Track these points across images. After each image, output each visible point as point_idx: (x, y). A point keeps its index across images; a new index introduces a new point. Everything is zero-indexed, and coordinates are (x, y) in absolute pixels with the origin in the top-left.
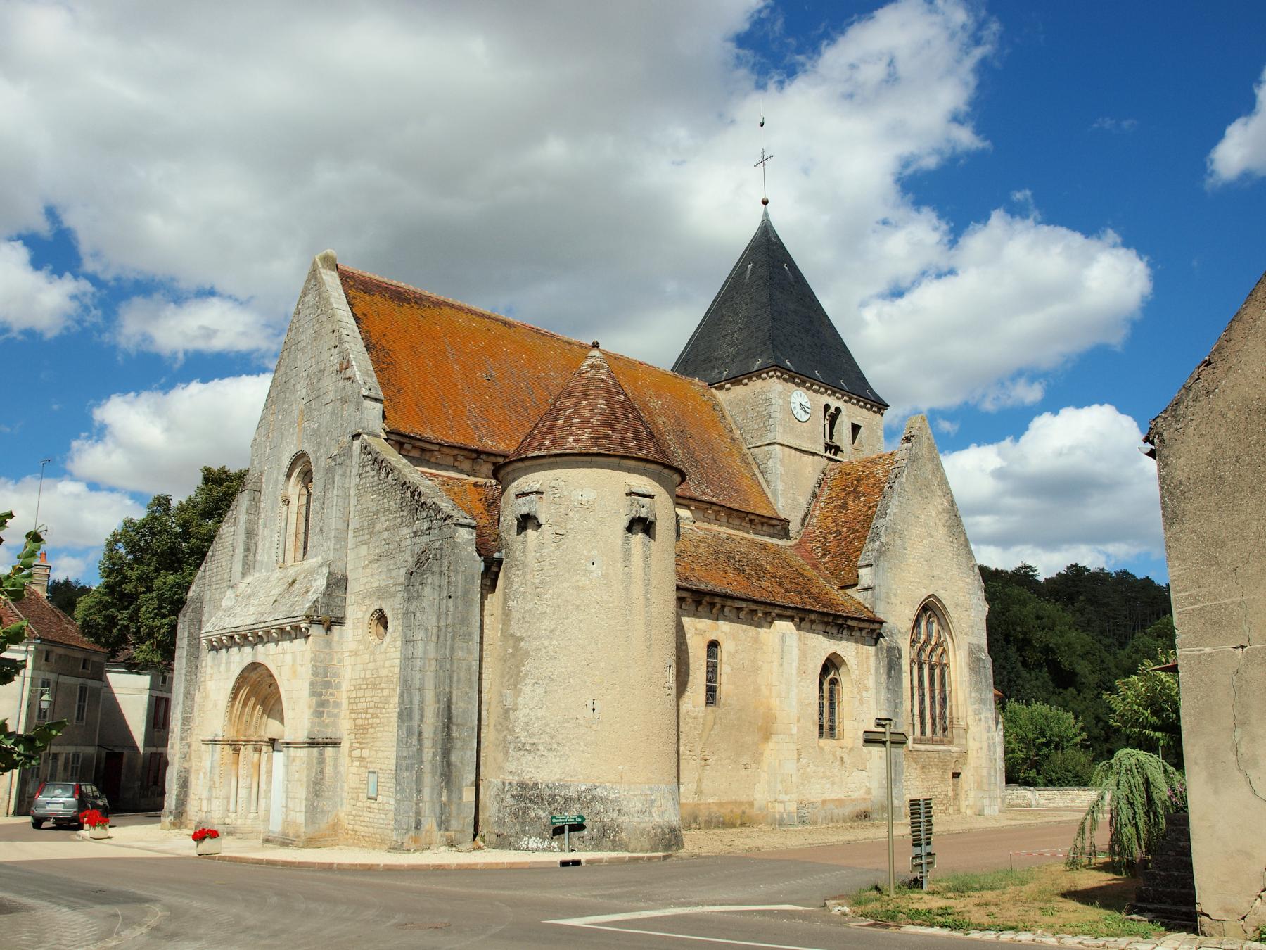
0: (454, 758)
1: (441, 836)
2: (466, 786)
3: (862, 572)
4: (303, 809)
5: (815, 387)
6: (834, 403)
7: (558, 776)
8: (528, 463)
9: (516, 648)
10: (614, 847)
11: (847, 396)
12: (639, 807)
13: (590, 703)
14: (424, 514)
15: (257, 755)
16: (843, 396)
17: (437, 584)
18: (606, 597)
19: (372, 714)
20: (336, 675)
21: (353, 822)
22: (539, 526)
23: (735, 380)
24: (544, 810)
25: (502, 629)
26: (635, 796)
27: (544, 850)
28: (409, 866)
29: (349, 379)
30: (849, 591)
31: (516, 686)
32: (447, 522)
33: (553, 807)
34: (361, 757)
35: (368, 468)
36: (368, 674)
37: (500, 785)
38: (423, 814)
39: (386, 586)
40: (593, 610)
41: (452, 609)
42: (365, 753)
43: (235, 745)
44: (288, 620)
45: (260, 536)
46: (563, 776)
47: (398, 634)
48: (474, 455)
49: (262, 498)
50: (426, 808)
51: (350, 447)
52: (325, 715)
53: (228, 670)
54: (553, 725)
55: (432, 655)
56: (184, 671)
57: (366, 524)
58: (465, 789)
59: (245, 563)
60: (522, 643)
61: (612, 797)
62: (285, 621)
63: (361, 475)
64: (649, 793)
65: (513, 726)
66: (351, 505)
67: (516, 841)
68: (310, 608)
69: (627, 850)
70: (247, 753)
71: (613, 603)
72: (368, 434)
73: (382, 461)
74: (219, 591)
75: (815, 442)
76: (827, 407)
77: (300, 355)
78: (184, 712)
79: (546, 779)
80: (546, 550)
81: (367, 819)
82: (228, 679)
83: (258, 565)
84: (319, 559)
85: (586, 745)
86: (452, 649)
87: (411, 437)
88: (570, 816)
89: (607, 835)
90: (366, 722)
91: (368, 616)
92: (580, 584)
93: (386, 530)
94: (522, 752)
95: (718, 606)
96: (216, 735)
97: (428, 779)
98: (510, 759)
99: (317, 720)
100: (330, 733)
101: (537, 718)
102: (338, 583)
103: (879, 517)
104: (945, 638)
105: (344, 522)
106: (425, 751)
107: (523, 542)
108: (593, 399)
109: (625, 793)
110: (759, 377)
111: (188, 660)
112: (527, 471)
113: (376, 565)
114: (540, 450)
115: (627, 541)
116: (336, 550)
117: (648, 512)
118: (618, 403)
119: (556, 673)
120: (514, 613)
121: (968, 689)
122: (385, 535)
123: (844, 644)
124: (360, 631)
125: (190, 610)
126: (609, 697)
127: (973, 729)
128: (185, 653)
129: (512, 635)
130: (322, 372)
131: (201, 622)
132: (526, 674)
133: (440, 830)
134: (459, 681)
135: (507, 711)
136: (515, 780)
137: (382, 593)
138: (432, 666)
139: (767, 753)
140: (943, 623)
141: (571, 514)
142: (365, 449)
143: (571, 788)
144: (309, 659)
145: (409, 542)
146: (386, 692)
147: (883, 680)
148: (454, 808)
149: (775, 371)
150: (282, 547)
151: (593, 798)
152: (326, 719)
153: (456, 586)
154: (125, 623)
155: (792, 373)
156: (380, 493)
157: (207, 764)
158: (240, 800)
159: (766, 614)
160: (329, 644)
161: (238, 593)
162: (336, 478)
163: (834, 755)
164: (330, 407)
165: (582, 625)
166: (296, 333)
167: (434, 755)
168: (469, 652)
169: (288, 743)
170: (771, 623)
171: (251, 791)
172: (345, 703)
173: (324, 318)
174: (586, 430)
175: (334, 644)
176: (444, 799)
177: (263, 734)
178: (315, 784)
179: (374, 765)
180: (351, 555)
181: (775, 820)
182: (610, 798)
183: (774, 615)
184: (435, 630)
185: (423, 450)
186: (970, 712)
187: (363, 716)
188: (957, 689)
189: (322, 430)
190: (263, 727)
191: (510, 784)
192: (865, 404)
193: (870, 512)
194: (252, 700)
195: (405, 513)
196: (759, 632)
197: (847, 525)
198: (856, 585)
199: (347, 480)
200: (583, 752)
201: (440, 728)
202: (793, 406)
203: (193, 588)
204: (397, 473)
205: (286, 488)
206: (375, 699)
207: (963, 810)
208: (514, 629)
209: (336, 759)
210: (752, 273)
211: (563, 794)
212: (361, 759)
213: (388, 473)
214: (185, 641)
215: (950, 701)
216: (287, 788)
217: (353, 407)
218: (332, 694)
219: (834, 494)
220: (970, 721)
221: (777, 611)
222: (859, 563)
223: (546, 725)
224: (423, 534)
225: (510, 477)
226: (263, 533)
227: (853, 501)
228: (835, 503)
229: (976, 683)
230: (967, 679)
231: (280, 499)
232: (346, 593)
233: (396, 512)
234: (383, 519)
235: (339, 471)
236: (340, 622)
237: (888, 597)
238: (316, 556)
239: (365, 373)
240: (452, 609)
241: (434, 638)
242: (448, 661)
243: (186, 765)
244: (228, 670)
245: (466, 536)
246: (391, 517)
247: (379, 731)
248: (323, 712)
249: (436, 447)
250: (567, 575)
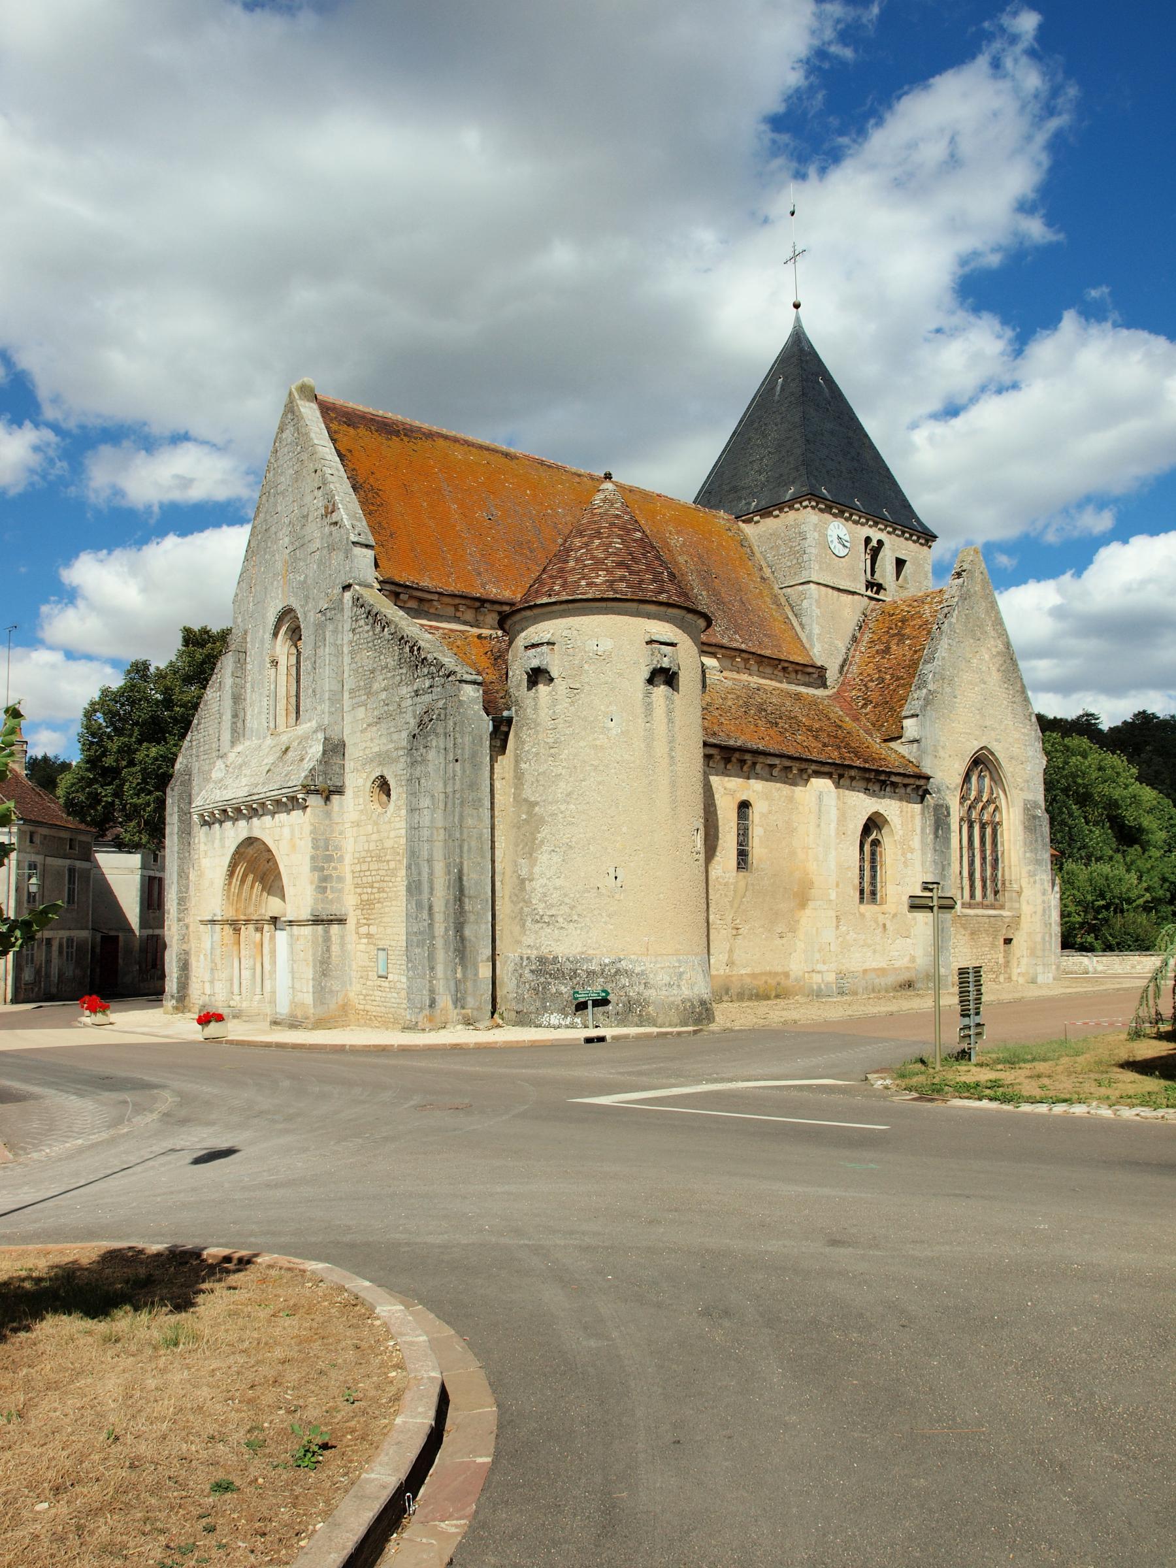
0: (468, 932)
1: (457, 1014)
2: (482, 961)
3: (907, 723)
4: (311, 990)
5: (854, 517)
6: (876, 535)
7: (579, 949)
8: (536, 611)
9: (530, 813)
10: (641, 1022)
11: (891, 526)
12: (667, 979)
13: (611, 871)
14: (426, 670)
15: (258, 935)
16: (886, 526)
17: (442, 746)
18: (626, 757)
19: (379, 888)
20: (338, 848)
21: (364, 1002)
22: (552, 680)
23: (765, 512)
24: (566, 985)
25: (514, 794)
26: (662, 968)
27: (567, 1027)
28: (425, 1046)
29: (336, 523)
30: (892, 745)
31: (531, 855)
32: (450, 679)
33: (575, 982)
34: (368, 934)
35: (362, 623)
36: (372, 846)
37: (517, 959)
38: (437, 992)
39: (387, 751)
40: (613, 771)
41: (459, 773)
42: (373, 930)
43: (235, 925)
44: (284, 791)
45: (248, 701)
46: (585, 949)
47: (402, 802)
48: (478, 604)
49: (248, 659)
50: (440, 986)
51: (341, 600)
52: (328, 891)
53: (223, 846)
54: (572, 895)
55: (440, 823)
56: (176, 849)
57: (362, 684)
58: (480, 965)
59: (234, 731)
60: (537, 809)
61: (638, 970)
62: (280, 792)
63: (354, 630)
64: (677, 964)
65: (530, 897)
66: (345, 664)
67: (537, 1017)
68: (306, 777)
69: (655, 1025)
70: (248, 932)
71: (634, 762)
72: (360, 585)
73: (377, 614)
74: (207, 762)
75: (855, 580)
76: (868, 540)
77: (280, 499)
78: (180, 891)
79: (567, 952)
81: (378, 999)
82: (223, 855)
83: (247, 732)
84: (314, 724)
85: (609, 916)
86: (461, 817)
87: (407, 587)
88: (594, 990)
89: (633, 1010)
90: (372, 897)
91: (369, 783)
92: (598, 743)
93: (385, 690)
94: (541, 925)
95: (749, 762)
96: (215, 915)
97: (440, 955)
98: (527, 933)
99: (320, 896)
100: (335, 910)
101: (555, 888)
102: (335, 749)
103: (926, 662)
104: (998, 794)
105: (339, 682)
106: (437, 925)
107: (534, 699)
108: (607, 538)
109: (652, 965)
110: (791, 507)
111: (180, 837)
112: (536, 620)
113: (375, 728)
114: (550, 595)
115: (648, 694)
116: (331, 713)
117: (670, 662)
118: (635, 541)
119: (574, 839)
120: (527, 776)
121: (1023, 849)
122: (383, 695)
123: (887, 801)
124: (361, 800)
125: (178, 784)
126: (632, 864)
127: (1027, 893)
128: (176, 830)
129: (526, 800)
130: (306, 517)
131: (190, 795)
132: (542, 842)
133: (456, 1008)
134: (469, 850)
135: (523, 881)
136: (534, 954)
137: (383, 758)
138: (441, 835)
139: (803, 921)
140: (996, 778)
141: (586, 667)
142: (358, 601)
143: (594, 962)
144: (308, 832)
145: (409, 702)
146: (392, 865)
147: (929, 840)
148: (469, 984)
149: (809, 500)
150: (272, 712)
151: (618, 972)
152: (330, 895)
153: (463, 749)
154: (109, 799)
155: (828, 503)
156: (375, 650)
157: (208, 945)
158: (244, 982)
159: (802, 771)
160: (328, 815)
161: (228, 763)
162: (328, 634)
163: (876, 922)
164: (317, 555)
165: (601, 787)
166: (274, 475)
167: (447, 930)
168: (480, 819)
169: (290, 922)
170: (807, 781)
171: (254, 972)
172: (348, 877)
173: (305, 456)
174: (600, 573)
175: (335, 815)
176: (459, 975)
177: (263, 911)
178: (322, 963)
179: (383, 942)
180: (348, 718)
181: (813, 991)
182: (636, 971)
183: (810, 771)
184: (442, 796)
185: (421, 600)
186: (1024, 874)
187: (369, 890)
188: (1010, 850)
189: (309, 582)
190: (264, 905)
191: (528, 958)
192: (911, 535)
193: (916, 657)
194: (251, 877)
195: (404, 671)
196: (793, 792)
197: (891, 671)
198: (900, 737)
199: (340, 636)
200: (606, 923)
201: (451, 901)
202: (830, 539)
203: (180, 759)
204: (393, 627)
205: (274, 648)
206: (381, 872)
207: (1014, 978)
208: (528, 793)
209: (342, 937)
210: (783, 389)
211: (585, 968)
212: (369, 936)
213: (384, 627)
214: (175, 818)
215: (1003, 862)
216: (293, 968)
217: (341, 556)
218: (335, 869)
219: (876, 638)
220: (1024, 883)
221: (814, 767)
222: (904, 714)
223: (566, 895)
224: (425, 693)
225: (518, 627)
226: (251, 698)
227: (898, 645)
228: (877, 647)
229: (1031, 843)
230: (1021, 838)
231: (268, 660)
232: (344, 759)
233: (394, 670)
234: (381, 677)
235: (330, 627)
236: (339, 791)
237: (936, 751)
238: (310, 720)
239: (353, 516)
240: (459, 773)
241: (442, 805)
242: (458, 829)
243: (185, 947)
244: (223, 846)
245: (472, 694)
246: (389, 675)
247: (387, 906)
248: (326, 887)
249: (436, 597)
250: (583, 733)
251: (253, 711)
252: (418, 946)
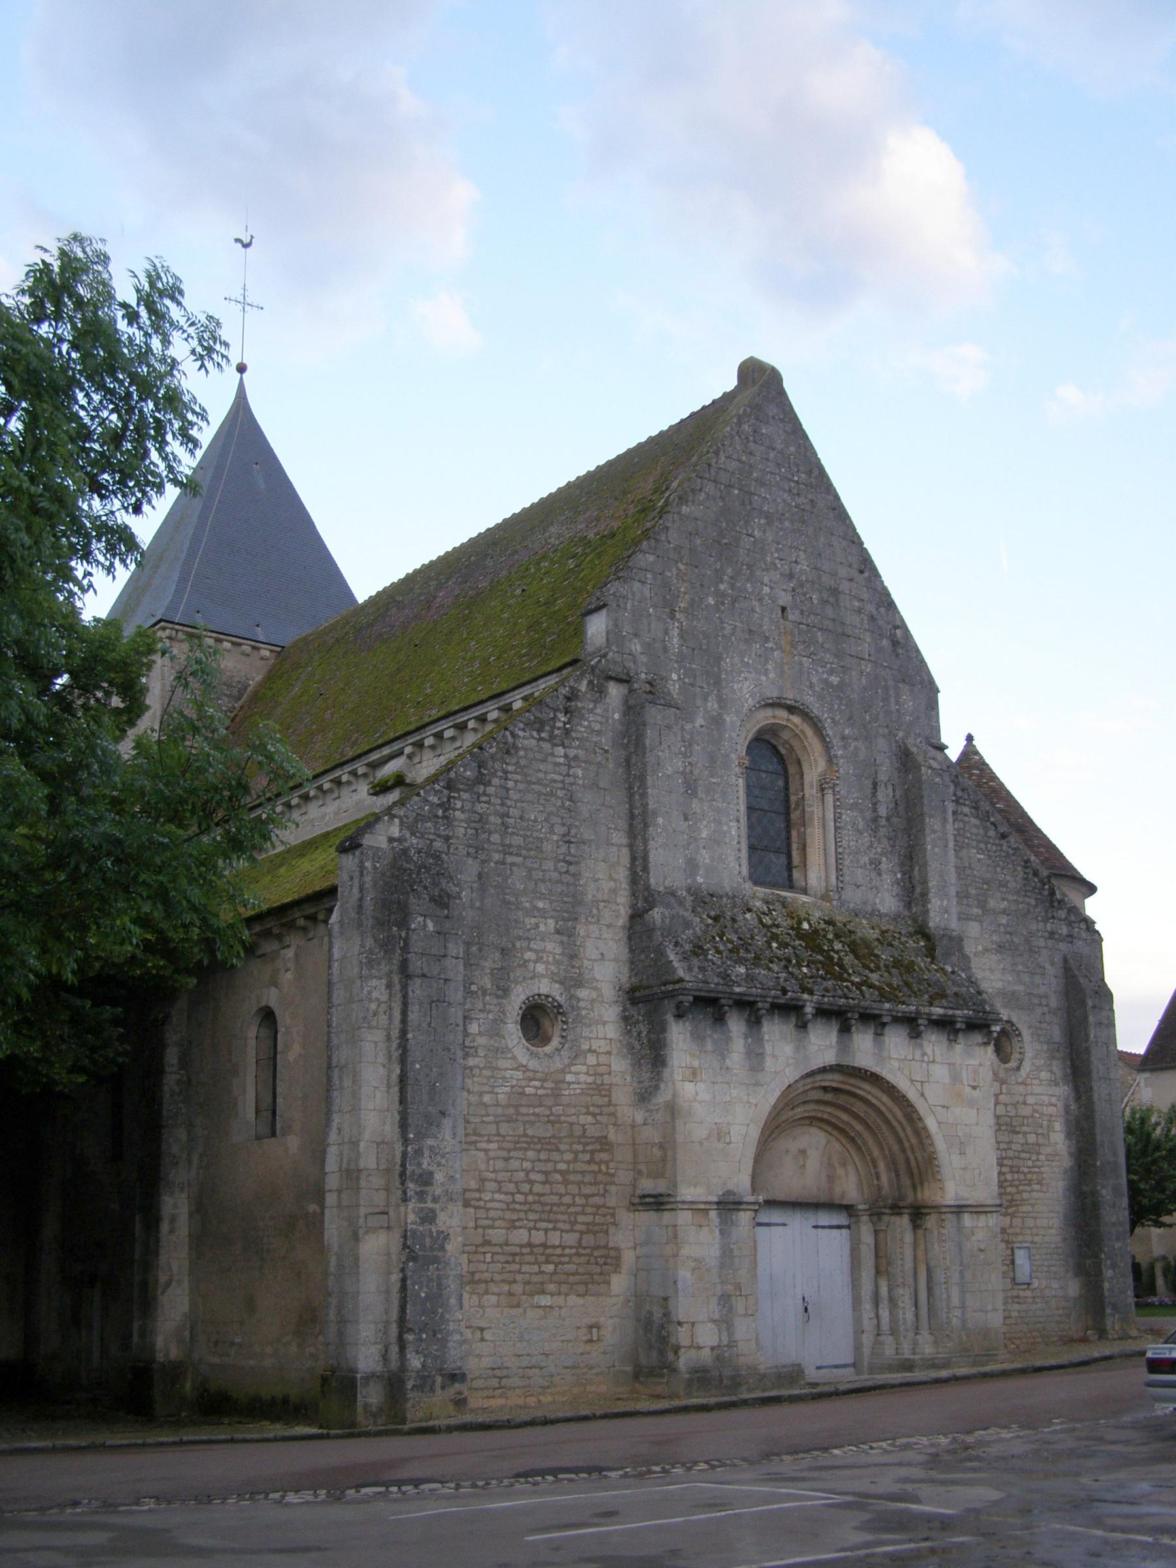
19: (1011, 1167)
93: (1004, 912)
145: (1042, 943)
252: (1118, 1239)
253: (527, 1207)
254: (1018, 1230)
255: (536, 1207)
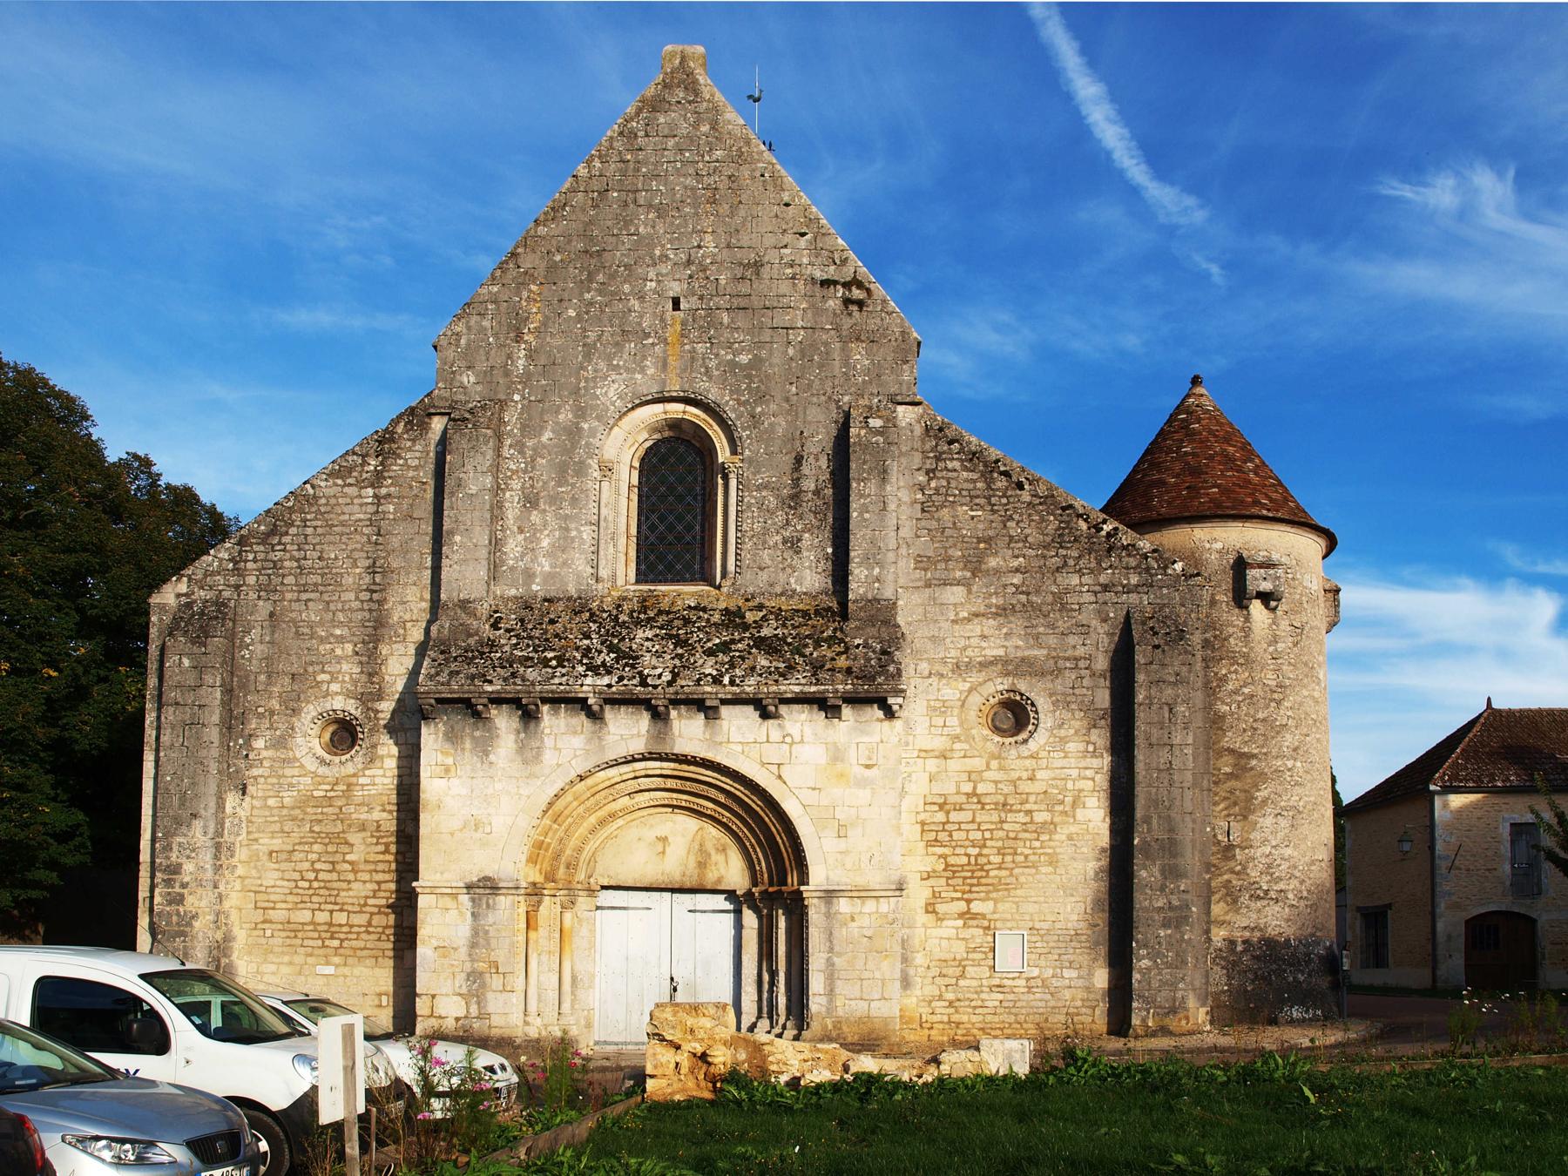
80: (1283, 645)
146: (1040, 817)
189: (766, 368)
251: (533, 539)
253: (311, 892)
254: (1009, 917)
255: (322, 892)
